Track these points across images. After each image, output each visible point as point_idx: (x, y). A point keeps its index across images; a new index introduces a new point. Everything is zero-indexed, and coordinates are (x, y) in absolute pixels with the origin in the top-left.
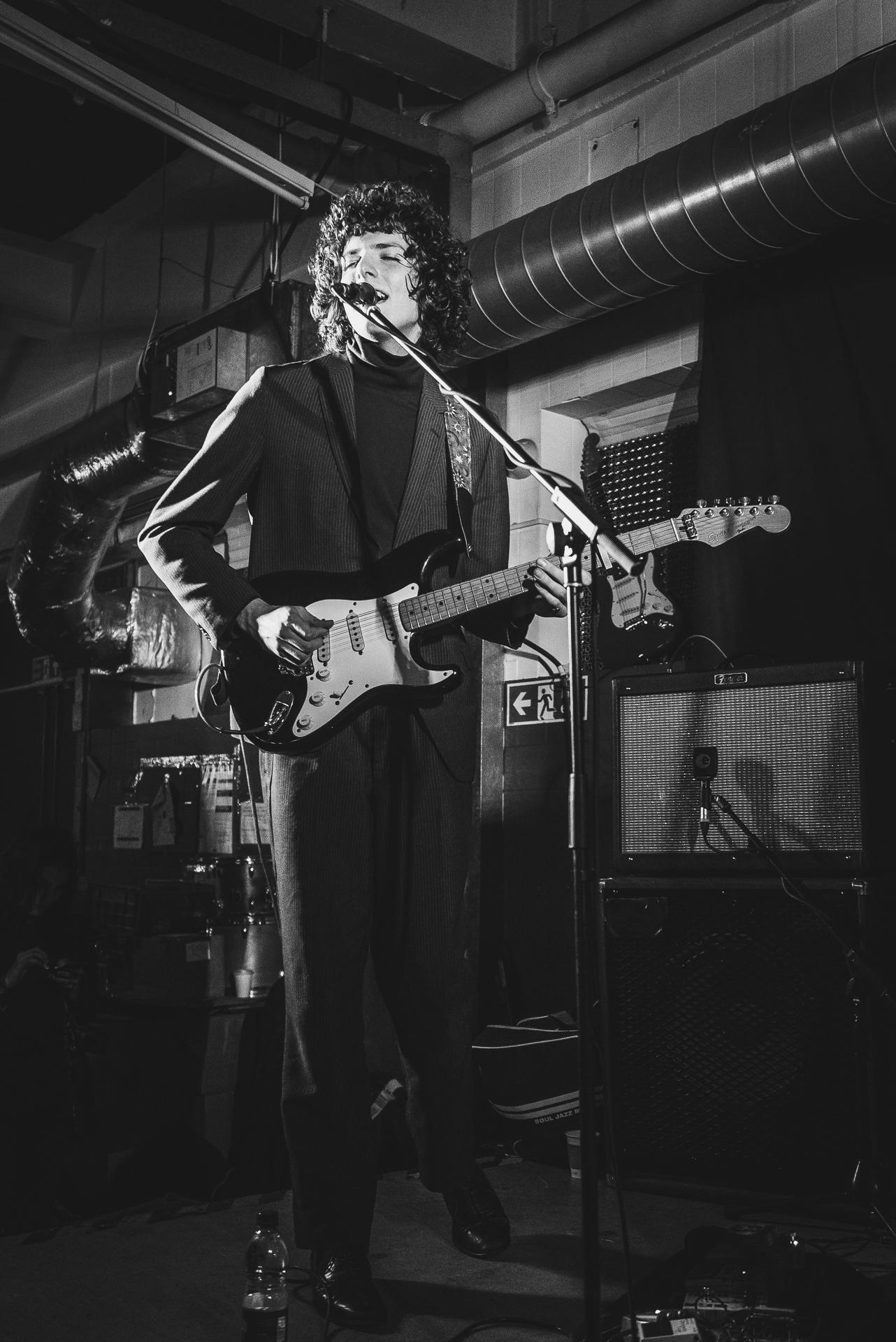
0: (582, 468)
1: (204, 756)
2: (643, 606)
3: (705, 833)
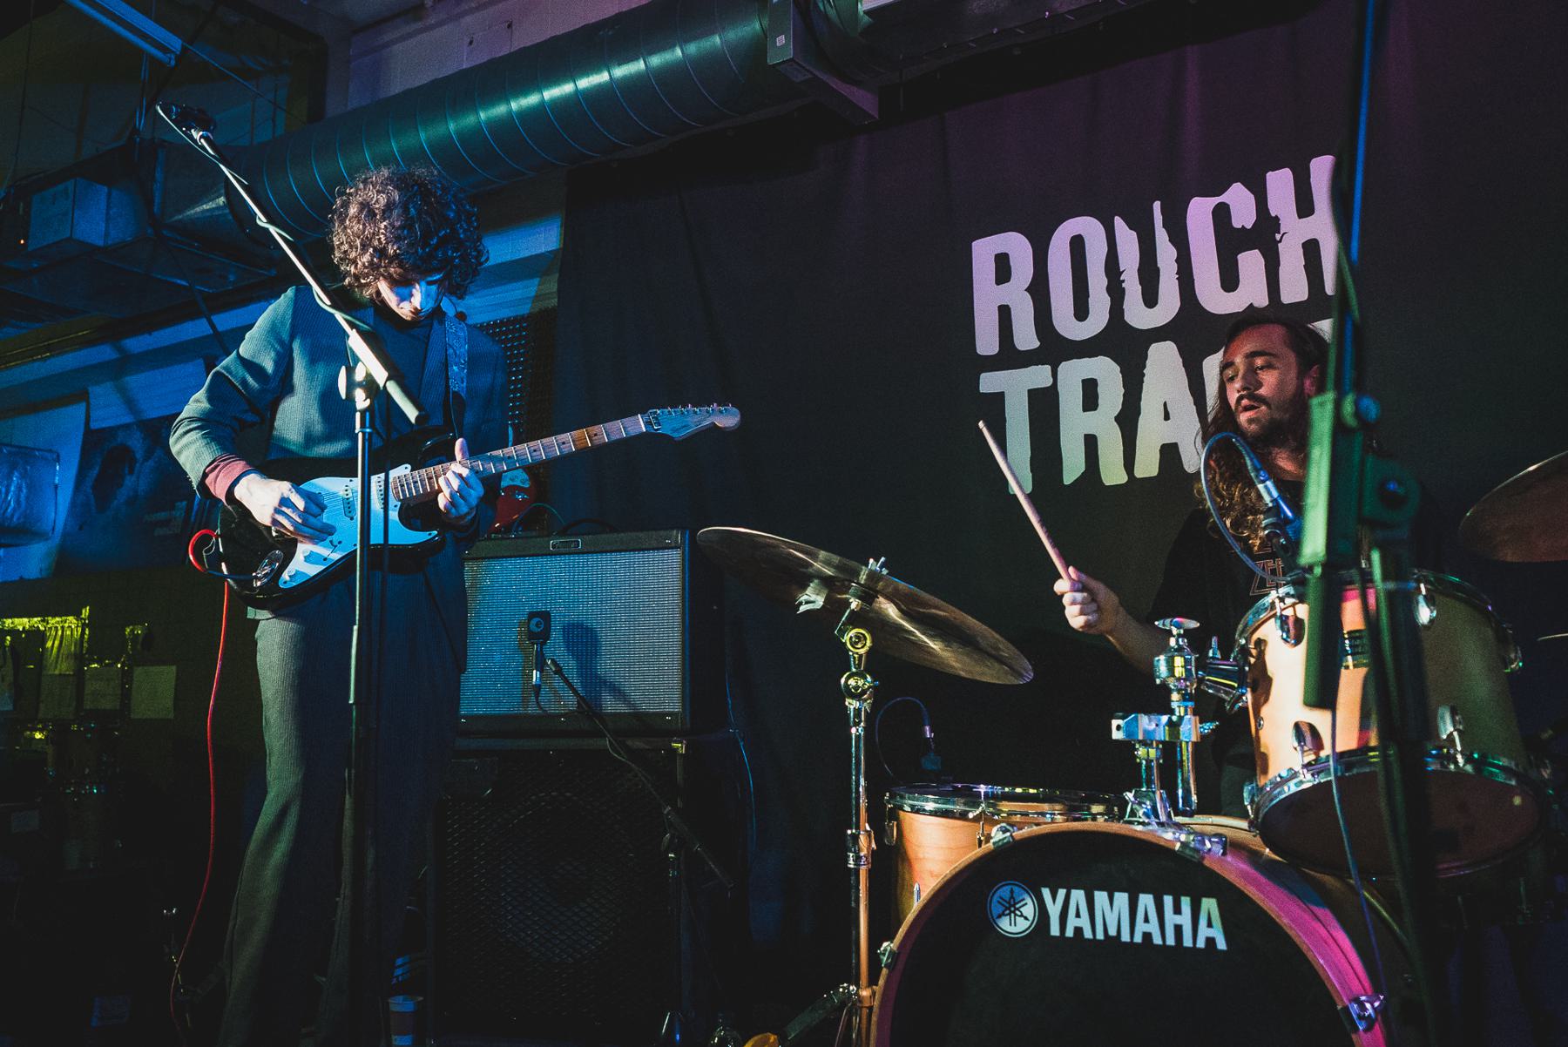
1: (50, 618)
3: (537, 695)
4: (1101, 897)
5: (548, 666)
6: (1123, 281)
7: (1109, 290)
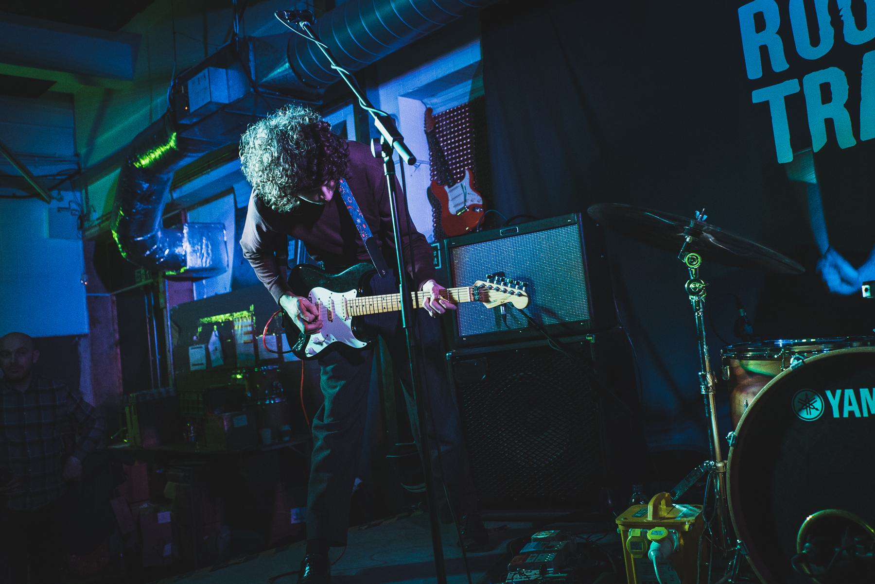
0: (425, 127)
1: (234, 313)
2: (465, 201)
4: (864, 392)
6: (842, 16)
7: (832, 23)
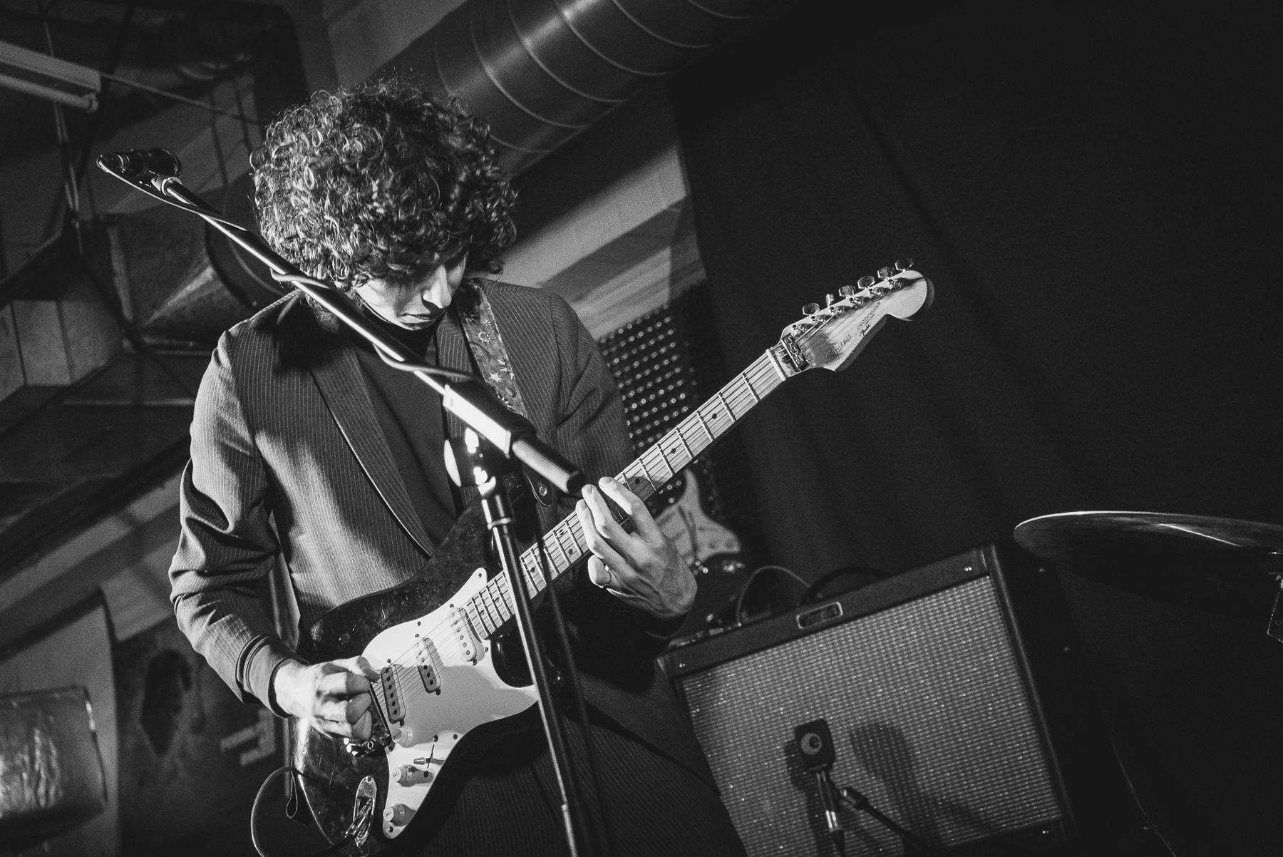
2: (695, 548)
5: (844, 799)
